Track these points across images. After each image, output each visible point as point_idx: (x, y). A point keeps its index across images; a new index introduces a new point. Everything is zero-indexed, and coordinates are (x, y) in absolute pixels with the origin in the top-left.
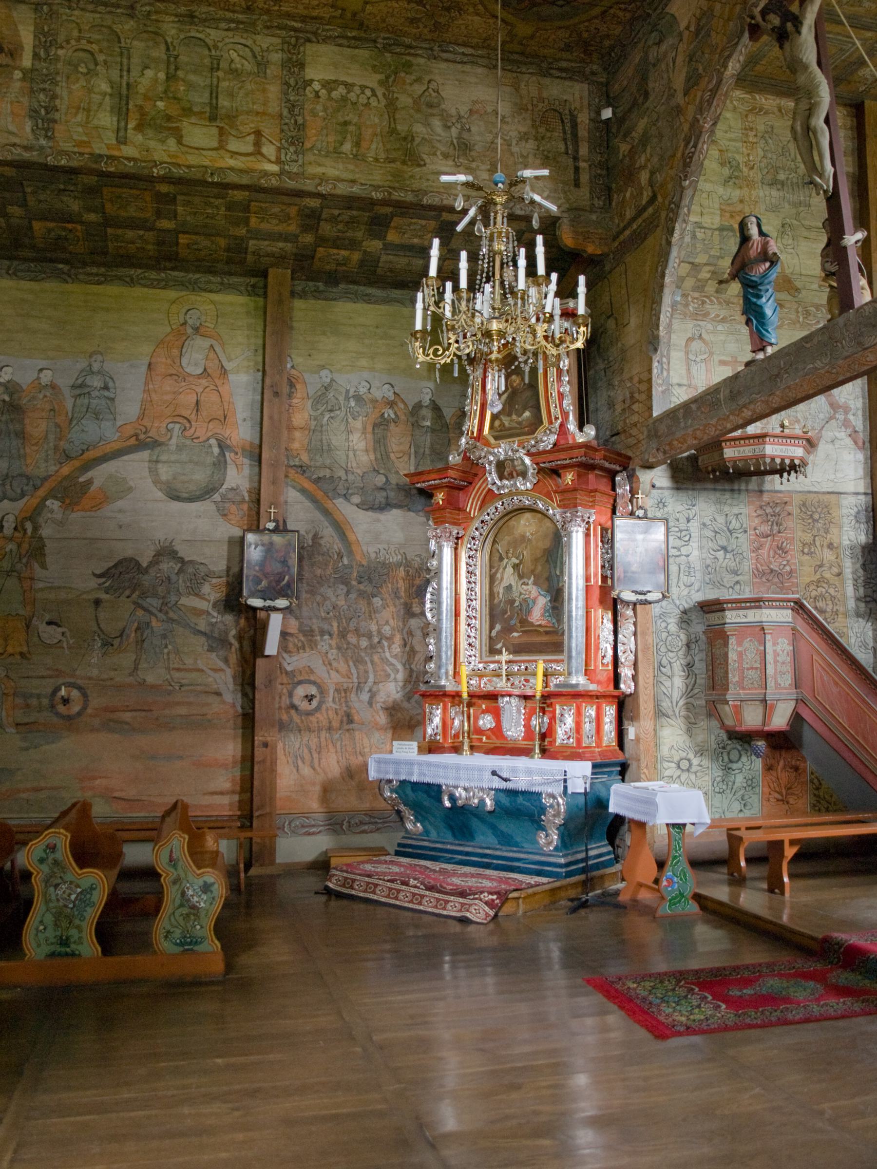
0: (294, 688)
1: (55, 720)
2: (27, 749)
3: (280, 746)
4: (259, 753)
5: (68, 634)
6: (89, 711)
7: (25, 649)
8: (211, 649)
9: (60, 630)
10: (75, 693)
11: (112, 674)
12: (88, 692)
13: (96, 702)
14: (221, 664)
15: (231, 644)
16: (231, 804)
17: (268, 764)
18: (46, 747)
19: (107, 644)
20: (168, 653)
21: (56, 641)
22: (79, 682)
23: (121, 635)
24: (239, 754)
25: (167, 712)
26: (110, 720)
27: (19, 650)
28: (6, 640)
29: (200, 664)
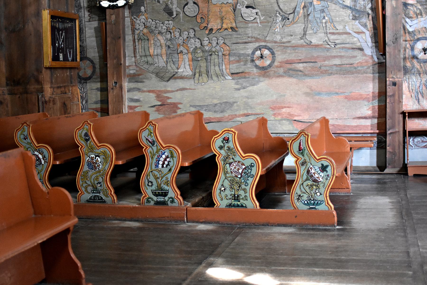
0: (416, 43)
1: (255, 70)
2: (239, 89)
3: (405, 86)
4: (390, 90)
5: (260, 13)
6: (276, 64)
7: (234, 25)
8: (355, 18)
9: (254, 11)
10: (266, 52)
11: (289, 38)
12: (274, 50)
13: (280, 57)
14: (363, 29)
15: (368, 14)
16: (372, 125)
17: (397, 97)
18: (250, 88)
19: (285, 18)
20: (326, 23)
21: (253, 18)
22: (269, 45)
23: (294, 12)
24: (377, 91)
25: (327, 63)
26: (290, 69)
27: (230, 26)
28: (222, 19)
29: (348, 29)
